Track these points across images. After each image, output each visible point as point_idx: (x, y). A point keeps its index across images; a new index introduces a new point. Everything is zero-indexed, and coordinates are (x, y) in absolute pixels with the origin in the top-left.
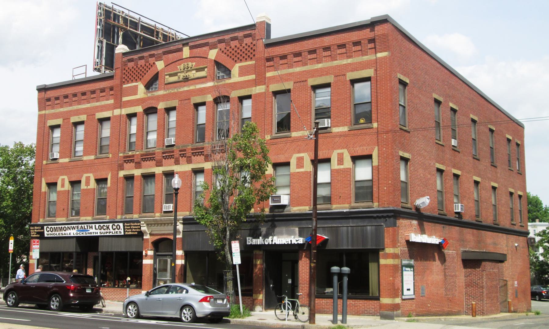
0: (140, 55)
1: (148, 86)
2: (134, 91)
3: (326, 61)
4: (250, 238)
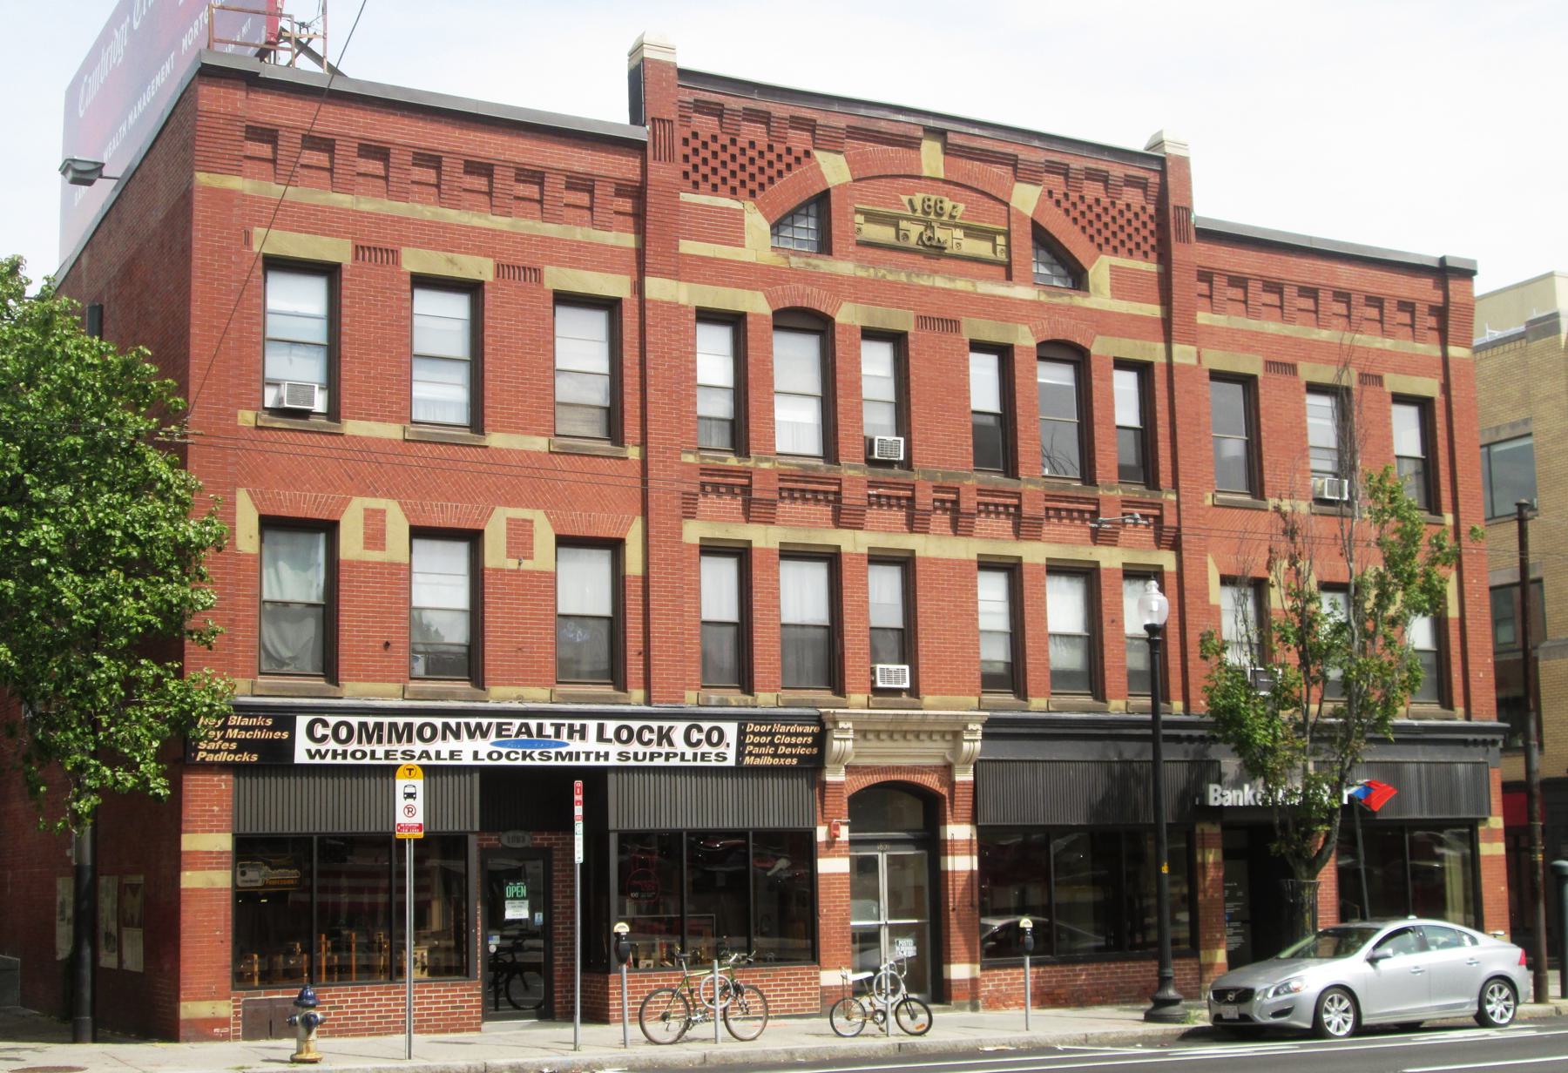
0: (1056, 158)
1: (776, 228)
2: (731, 230)
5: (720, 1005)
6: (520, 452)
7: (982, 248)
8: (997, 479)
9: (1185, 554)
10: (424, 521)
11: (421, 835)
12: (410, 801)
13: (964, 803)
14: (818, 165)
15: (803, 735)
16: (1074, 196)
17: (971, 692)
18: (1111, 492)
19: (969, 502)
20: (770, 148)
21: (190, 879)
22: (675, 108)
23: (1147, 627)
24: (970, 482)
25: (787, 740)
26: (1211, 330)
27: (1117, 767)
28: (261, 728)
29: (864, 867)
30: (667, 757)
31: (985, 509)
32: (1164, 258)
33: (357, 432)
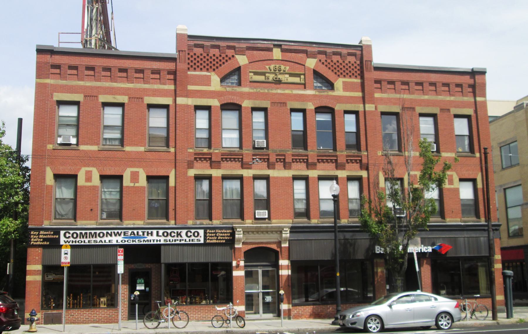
1: (222, 80)
2: (207, 81)
3: (431, 94)
4: (379, 247)
5: (170, 317)
6: (135, 152)
7: (296, 80)
8: (301, 151)
9: (370, 171)
10: (104, 173)
11: (69, 265)
12: (66, 255)
13: (285, 253)
14: (237, 59)
15: (226, 233)
16: (329, 61)
17: (290, 218)
18: (342, 153)
19: (289, 159)
20: (220, 56)
21: (29, 278)
22: (187, 47)
23: (333, 196)
24: (289, 153)
25: (221, 235)
26: (381, 99)
27: (343, 241)
28: (50, 235)
29: (249, 275)
30: (180, 241)
31: (294, 161)
32: (362, 77)
33: (84, 149)
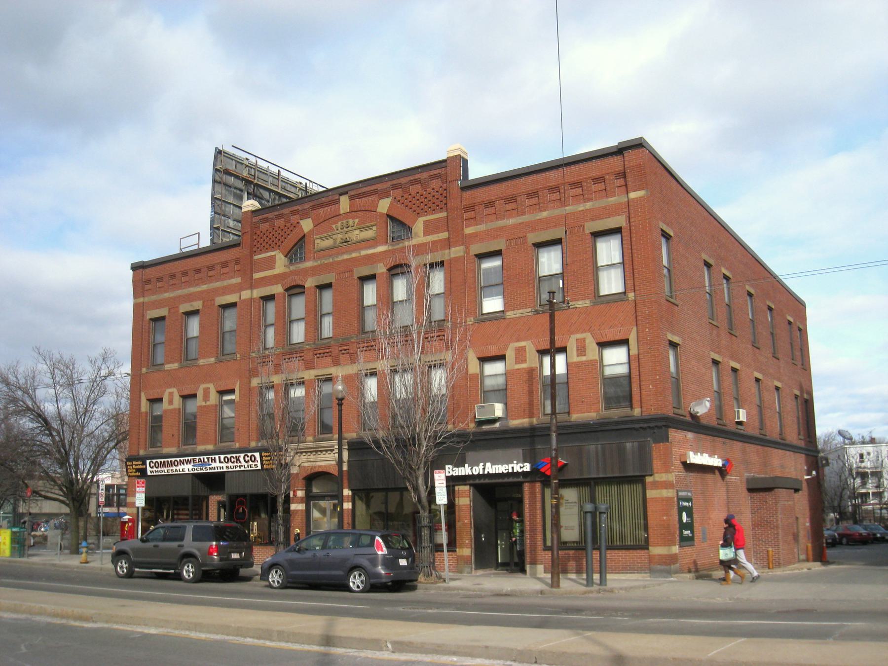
2: (270, 263)
3: (554, 208)
4: (451, 467)
